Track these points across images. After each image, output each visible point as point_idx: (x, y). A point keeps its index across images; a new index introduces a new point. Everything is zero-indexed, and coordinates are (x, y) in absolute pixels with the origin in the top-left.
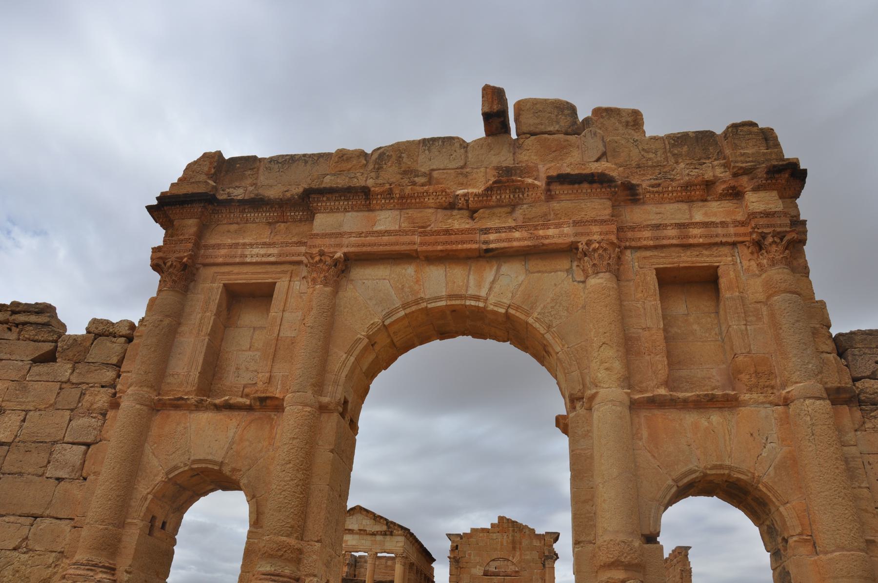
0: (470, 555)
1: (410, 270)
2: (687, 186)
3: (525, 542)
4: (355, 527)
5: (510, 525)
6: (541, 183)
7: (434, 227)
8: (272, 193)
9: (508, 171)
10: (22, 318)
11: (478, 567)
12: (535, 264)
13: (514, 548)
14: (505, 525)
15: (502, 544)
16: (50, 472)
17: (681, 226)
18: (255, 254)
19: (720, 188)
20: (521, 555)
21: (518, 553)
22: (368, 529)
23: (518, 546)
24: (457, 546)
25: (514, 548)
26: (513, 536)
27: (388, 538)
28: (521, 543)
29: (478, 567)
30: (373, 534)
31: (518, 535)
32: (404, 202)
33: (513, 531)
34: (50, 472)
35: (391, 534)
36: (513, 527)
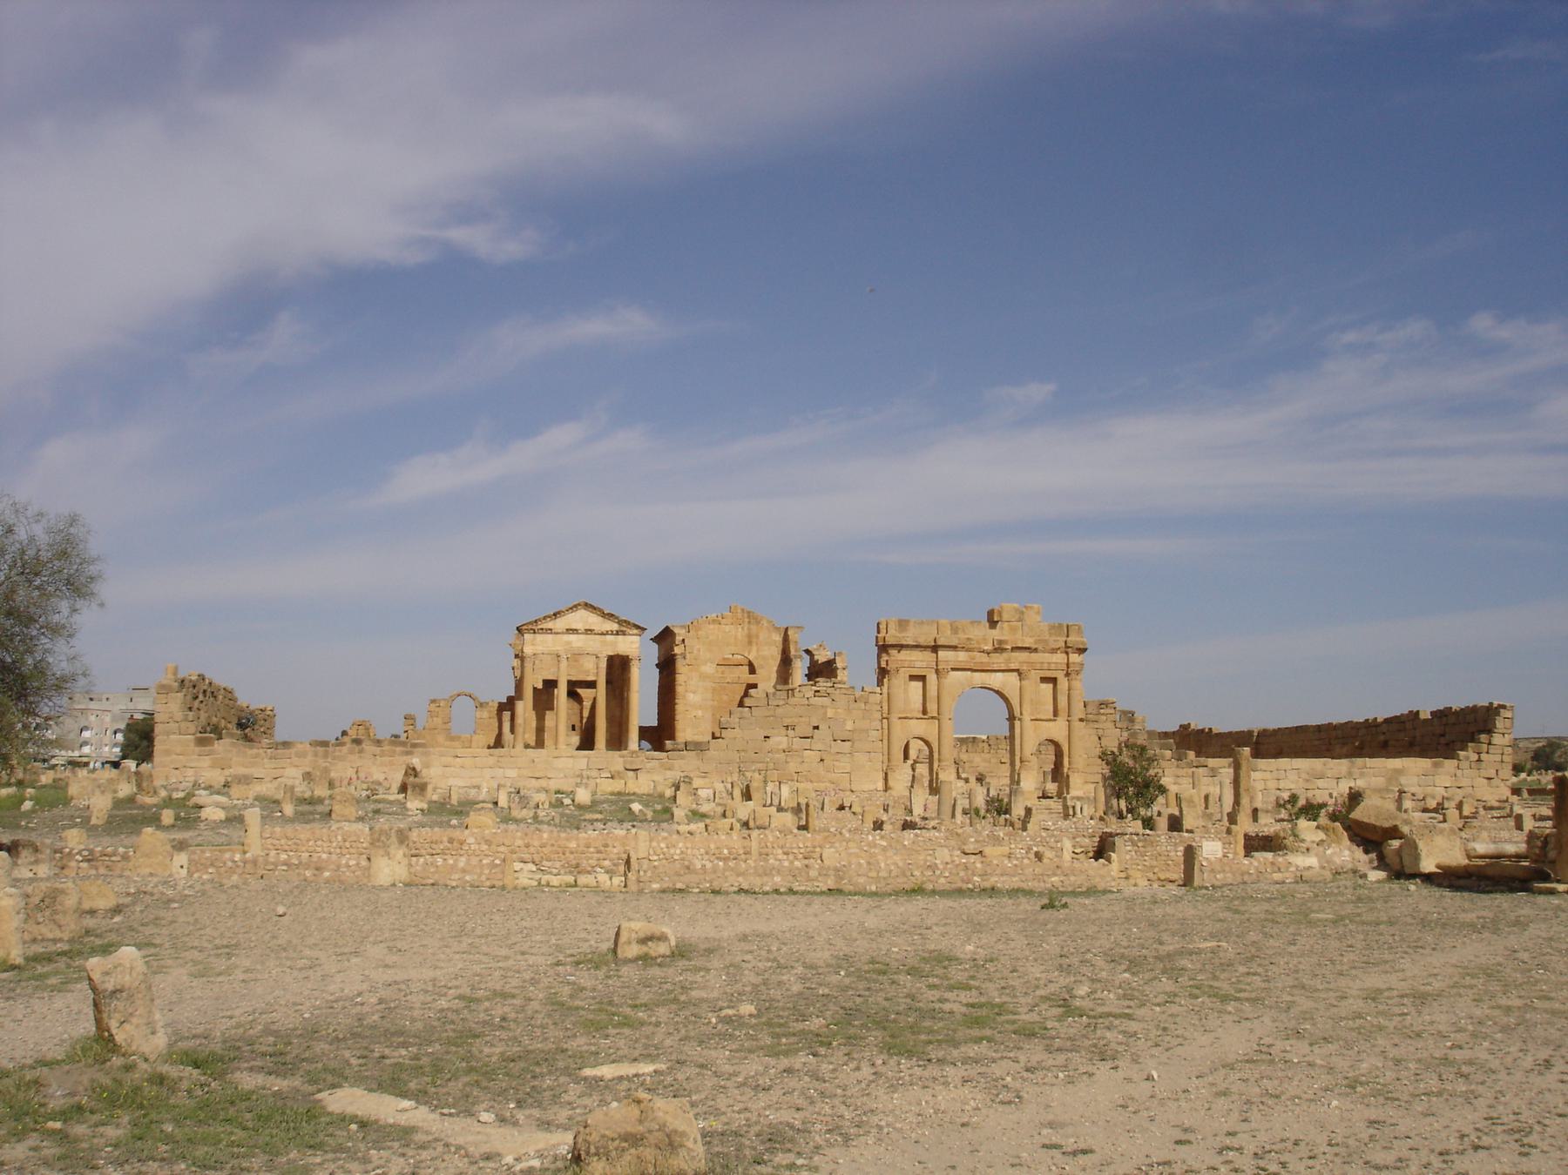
0: (699, 650)
1: (969, 672)
2: (1053, 649)
3: (763, 636)
4: (580, 626)
5: (746, 615)
6: (1009, 647)
7: (977, 660)
8: (922, 641)
9: (1000, 642)
10: (840, 686)
11: (709, 664)
12: (1006, 674)
13: (750, 643)
14: (740, 615)
15: (736, 638)
16: (870, 739)
17: (1049, 663)
18: (918, 664)
19: (1063, 649)
20: (758, 651)
21: (754, 648)
22: (597, 628)
23: (754, 640)
24: (683, 640)
25: (750, 643)
26: (749, 629)
27: (620, 637)
28: (757, 637)
29: (709, 664)
30: (602, 634)
31: (754, 628)
32: (969, 650)
33: (749, 622)
34: (870, 739)
35: (624, 633)
36: (749, 617)
